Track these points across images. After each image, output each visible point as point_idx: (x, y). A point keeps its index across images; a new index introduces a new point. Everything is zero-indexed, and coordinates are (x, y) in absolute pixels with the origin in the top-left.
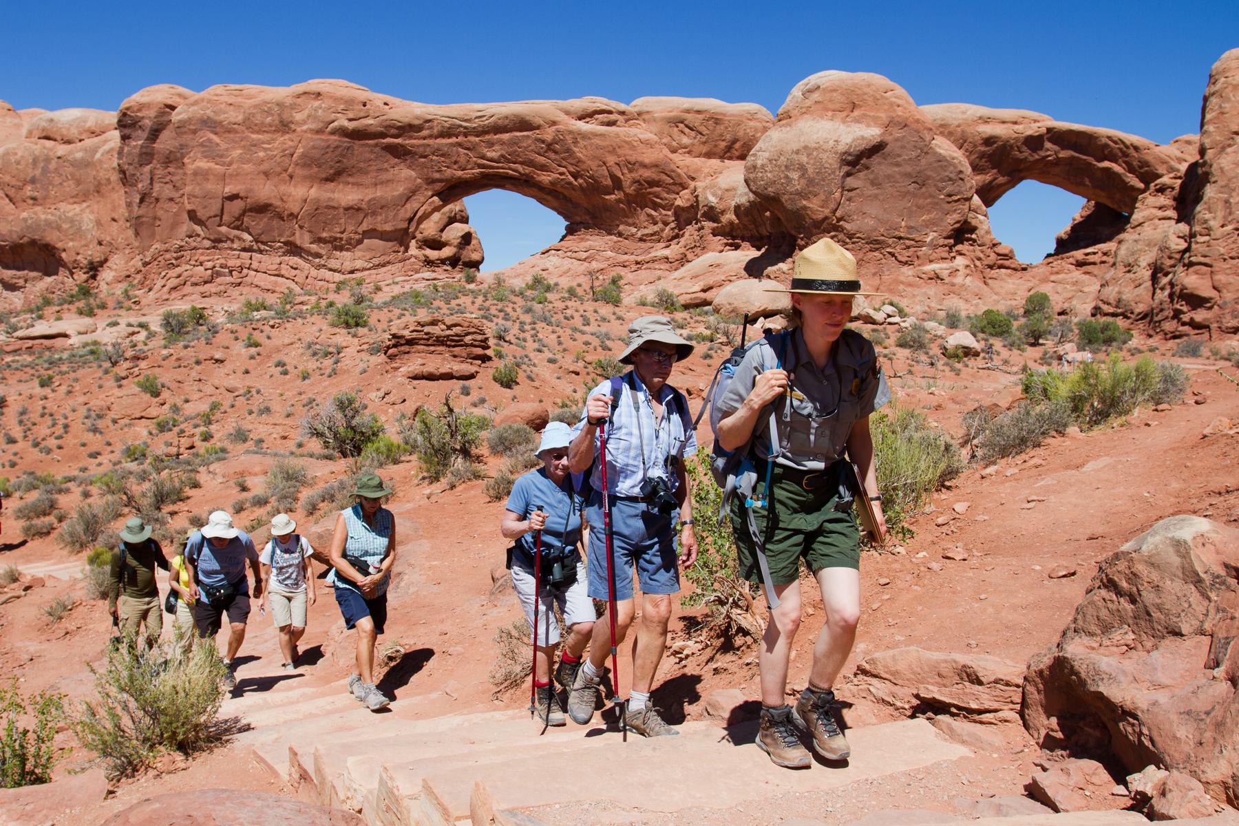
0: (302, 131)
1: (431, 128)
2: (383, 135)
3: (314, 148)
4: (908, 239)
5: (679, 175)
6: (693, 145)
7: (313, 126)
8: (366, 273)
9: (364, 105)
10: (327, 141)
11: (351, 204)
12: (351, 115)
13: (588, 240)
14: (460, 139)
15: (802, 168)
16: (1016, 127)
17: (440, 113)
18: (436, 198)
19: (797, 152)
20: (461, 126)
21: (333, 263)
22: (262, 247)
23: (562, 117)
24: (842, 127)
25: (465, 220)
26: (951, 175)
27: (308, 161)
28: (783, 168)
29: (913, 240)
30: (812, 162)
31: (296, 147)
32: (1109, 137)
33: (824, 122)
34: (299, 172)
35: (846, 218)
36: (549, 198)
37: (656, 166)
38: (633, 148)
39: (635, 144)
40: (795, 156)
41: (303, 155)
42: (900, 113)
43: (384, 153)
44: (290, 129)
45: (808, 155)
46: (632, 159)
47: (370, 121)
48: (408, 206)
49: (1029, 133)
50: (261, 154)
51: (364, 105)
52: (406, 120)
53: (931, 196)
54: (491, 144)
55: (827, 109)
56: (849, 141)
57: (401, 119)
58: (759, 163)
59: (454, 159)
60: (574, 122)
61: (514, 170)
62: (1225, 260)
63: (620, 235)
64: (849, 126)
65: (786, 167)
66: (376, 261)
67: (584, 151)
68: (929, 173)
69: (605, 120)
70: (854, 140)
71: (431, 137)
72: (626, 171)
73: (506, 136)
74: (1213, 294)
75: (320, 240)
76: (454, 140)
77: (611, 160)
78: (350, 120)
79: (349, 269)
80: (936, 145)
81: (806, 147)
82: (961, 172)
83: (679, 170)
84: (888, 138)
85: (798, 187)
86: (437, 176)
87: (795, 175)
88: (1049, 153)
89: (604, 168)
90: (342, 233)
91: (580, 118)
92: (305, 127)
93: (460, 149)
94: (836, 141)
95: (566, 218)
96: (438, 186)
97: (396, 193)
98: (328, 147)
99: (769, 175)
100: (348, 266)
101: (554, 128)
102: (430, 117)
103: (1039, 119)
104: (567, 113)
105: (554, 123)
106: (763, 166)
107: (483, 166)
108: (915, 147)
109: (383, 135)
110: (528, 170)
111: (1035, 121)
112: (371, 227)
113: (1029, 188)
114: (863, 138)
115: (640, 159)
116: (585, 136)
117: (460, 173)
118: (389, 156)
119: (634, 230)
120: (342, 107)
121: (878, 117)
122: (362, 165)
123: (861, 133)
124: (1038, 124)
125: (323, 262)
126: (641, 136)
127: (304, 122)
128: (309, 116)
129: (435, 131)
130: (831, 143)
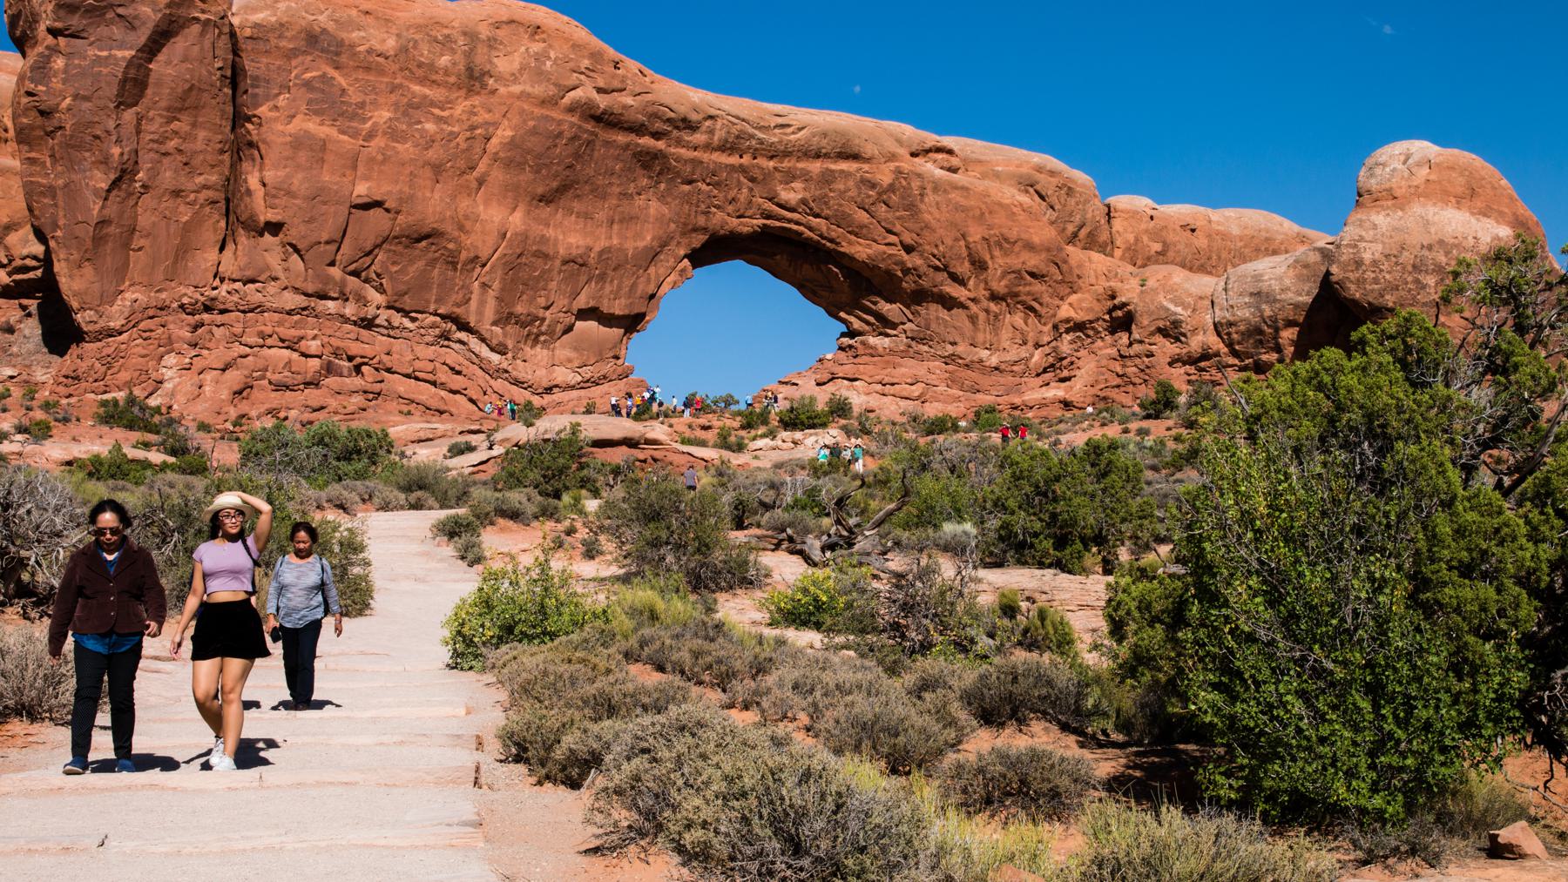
0: (511, 95)
1: (711, 132)
2: (638, 129)
3: (534, 132)
7: (539, 90)
10: (560, 123)
11: (574, 252)
13: (901, 365)
14: (746, 160)
19: (1430, 248)
20: (752, 136)
21: (521, 371)
22: (397, 319)
27: (516, 157)
28: (1410, 269)
31: (496, 125)
34: (498, 175)
40: (1426, 253)
41: (512, 144)
44: (484, 86)
45: (1447, 254)
46: (1013, 235)
47: (629, 101)
48: (652, 270)
50: (430, 127)
54: (790, 177)
57: (674, 107)
58: (1367, 256)
59: (732, 194)
61: (811, 229)
63: (950, 359)
65: (1414, 266)
66: (587, 372)
67: (933, 210)
71: (708, 147)
72: (997, 253)
73: (816, 167)
75: (504, 319)
76: (734, 160)
77: (976, 234)
78: (600, 90)
79: (545, 384)
81: (1441, 242)
86: (701, 221)
89: (962, 243)
92: (516, 89)
98: (560, 134)
99: (1388, 276)
100: (541, 376)
101: (892, 165)
102: (713, 112)
106: (1375, 263)
109: (638, 129)
110: (836, 232)
115: (1024, 236)
119: (984, 354)
125: (505, 365)
127: (514, 78)
128: (522, 69)
129: (716, 138)
130: (1471, 241)
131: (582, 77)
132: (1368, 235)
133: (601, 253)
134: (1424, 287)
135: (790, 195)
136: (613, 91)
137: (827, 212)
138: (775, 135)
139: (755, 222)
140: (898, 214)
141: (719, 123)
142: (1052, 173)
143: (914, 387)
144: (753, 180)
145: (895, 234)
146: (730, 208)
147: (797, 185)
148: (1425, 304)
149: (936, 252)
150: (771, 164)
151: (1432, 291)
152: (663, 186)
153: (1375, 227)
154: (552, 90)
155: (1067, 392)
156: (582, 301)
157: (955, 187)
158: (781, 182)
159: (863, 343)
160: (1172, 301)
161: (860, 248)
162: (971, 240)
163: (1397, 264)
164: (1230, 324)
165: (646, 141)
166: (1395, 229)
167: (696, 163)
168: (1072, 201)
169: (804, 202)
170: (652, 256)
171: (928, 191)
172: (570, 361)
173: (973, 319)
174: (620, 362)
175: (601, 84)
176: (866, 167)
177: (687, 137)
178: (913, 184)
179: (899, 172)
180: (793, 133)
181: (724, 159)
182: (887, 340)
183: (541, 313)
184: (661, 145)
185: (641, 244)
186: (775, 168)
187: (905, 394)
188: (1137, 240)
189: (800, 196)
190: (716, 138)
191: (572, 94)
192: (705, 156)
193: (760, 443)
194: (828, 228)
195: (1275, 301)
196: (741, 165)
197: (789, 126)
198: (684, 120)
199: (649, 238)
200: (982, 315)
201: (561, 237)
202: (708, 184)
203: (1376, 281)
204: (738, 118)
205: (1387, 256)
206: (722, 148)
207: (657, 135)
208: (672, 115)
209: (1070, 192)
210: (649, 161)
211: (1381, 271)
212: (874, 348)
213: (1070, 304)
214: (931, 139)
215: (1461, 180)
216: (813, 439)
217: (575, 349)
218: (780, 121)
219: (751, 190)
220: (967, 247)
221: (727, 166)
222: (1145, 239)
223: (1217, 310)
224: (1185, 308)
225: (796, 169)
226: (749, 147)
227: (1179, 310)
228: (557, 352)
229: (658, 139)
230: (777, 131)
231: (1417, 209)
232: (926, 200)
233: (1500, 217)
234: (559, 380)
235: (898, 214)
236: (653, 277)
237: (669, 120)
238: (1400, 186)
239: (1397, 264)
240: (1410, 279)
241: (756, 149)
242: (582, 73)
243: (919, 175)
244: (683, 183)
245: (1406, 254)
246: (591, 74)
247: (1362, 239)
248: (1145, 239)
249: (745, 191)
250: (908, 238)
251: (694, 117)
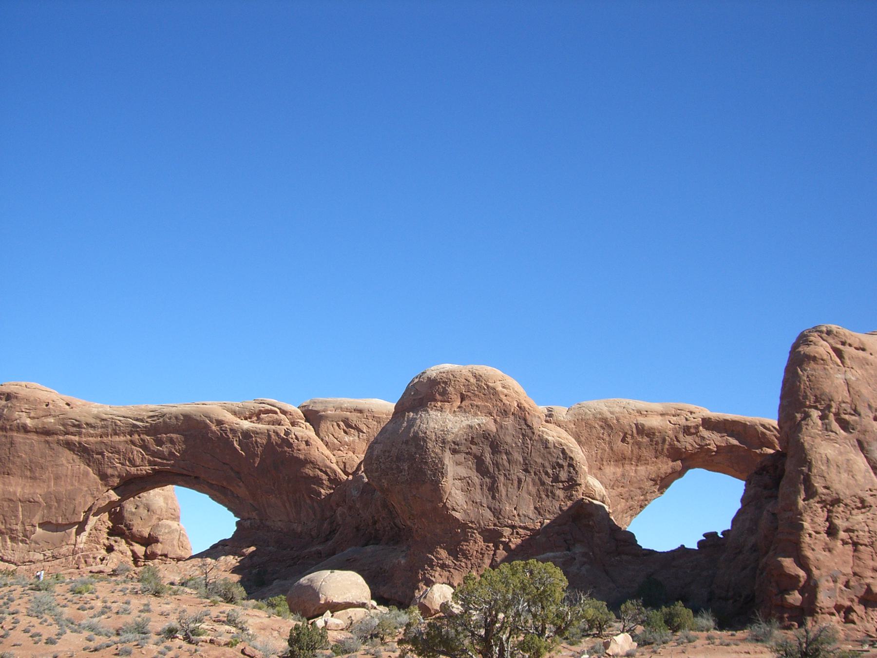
4: (520, 527)
5: (335, 472)
6: (354, 441)
8: (39, 564)
9: (47, 405)
12: (32, 415)
16: (674, 419)
17: (115, 412)
18: (111, 492)
23: (229, 417)
24: (450, 416)
25: (176, 518)
26: (560, 462)
29: (525, 528)
32: (763, 426)
33: (431, 412)
35: (456, 507)
36: (218, 494)
37: (312, 462)
38: (290, 445)
39: (291, 441)
40: (404, 446)
42: (506, 402)
43: (61, 449)
49: (683, 422)
51: (47, 405)
52: (83, 420)
53: (543, 483)
55: (436, 400)
56: (455, 430)
57: (78, 418)
60: (239, 420)
62: (810, 535)
64: (456, 416)
68: (539, 460)
69: (270, 419)
70: (460, 429)
74: (802, 573)
80: (543, 432)
82: (571, 458)
83: (334, 466)
84: (493, 427)
88: (708, 442)
90: (17, 524)
91: (246, 419)
93: (133, 447)
94: (442, 431)
95: (236, 515)
96: (116, 481)
97: (70, 488)
102: (105, 416)
103: (694, 410)
104: (235, 413)
105: (220, 423)
107: (155, 464)
108: (523, 435)
111: (691, 413)
112: (46, 520)
113: (697, 476)
114: (471, 427)
116: (247, 434)
117: (133, 470)
118: (67, 453)
120: (27, 406)
121: (485, 406)
122: (42, 461)
123: (469, 423)
124: (694, 415)
126: (299, 434)
138: (147, 422)
148: (402, 483)
178: (231, 436)
181: (117, 439)
183: (14, 527)
184: (77, 438)
192: (105, 439)
198: (87, 424)
202: (112, 453)
204: (124, 417)
210: (69, 445)
218: (151, 414)
230: (149, 420)
234: (31, 558)
237: (74, 426)
239: (389, 457)
240: (394, 466)
242: (22, 412)
249: (135, 453)
251: (92, 421)
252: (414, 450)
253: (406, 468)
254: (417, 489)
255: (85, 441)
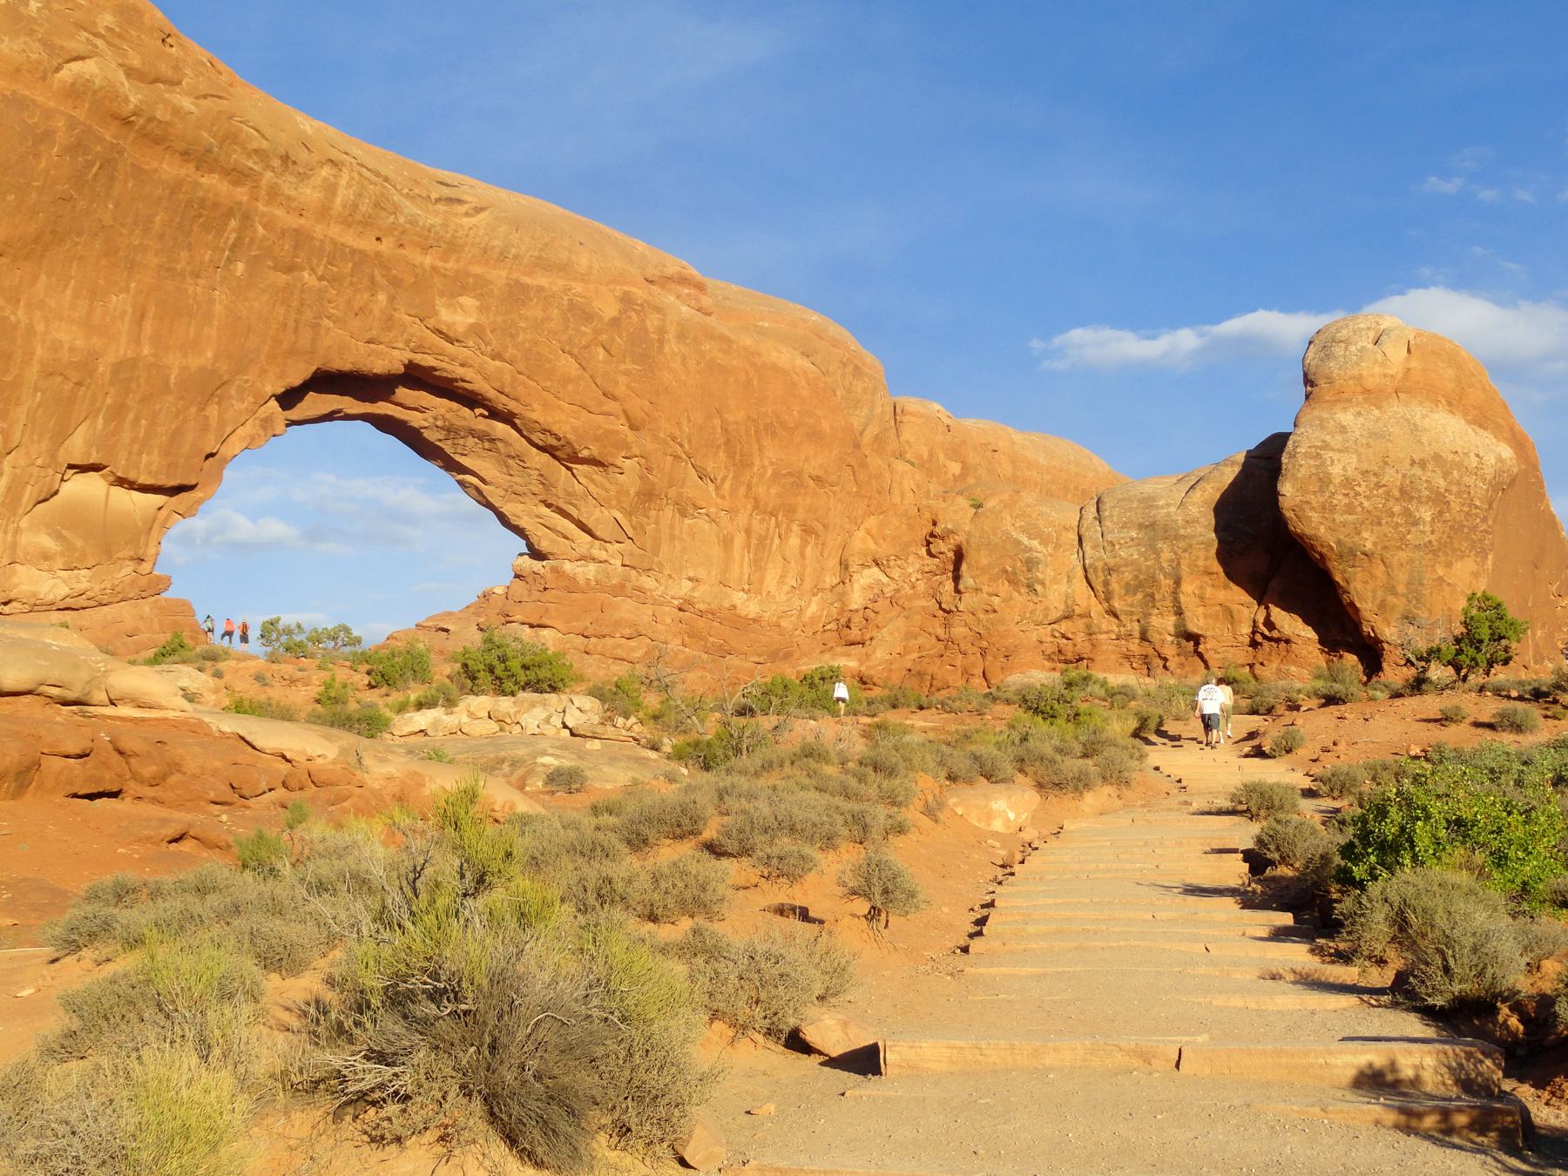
1: (331, 189)
2: (203, 159)
10: (48, 114)
14: (386, 247)
15: (1438, 500)
19: (1423, 464)
28: (1396, 493)
30: (1454, 489)
40: (1417, 471)
45: (1446, 475)
47: (187, 103)
57: (268, 131)
58: (1336, 470)
65: (1402, 490)
66: (82, 580)
81: (1437, 457)
85: (1433, 538)
87: (1426, 514)
89: (717, 422)
99: (1366, 504)
106: (1348, 482)
109: (203, 159)
130: (1474, 461)
131: (99, 42)
132: (1336, 441)
133: (117, 368)
134: (1416, 523)
135: (460, 315)
136: (156, 80)
137: (510, 352)
138: (437, 213)
139: (396, 353)
140: (623, 367)
141: (344, 179)
142: (835, 343)
143: (633, 643)
144: (396, 282)
145: (614, 398)
146: (356, 323)
147: (468, 301)
148: (1417, 547)
149: (677, 433)
150: (428, 261)
151: (1428, 528)
152: (240, 267)
153: (1343, 429)
154: (37, 53)
155: (861, 662)
156: (77, 447)
157: (711, 336)
158: (442, 294)
159: (555, 570)
160: (1023, 530)
161: (563, 417)
162: (730, 418)
163: (1378, 486)
164: (1109, 570)
165: (212, 182)
166: (1372, 435)
167: (300, 238)
168: (859, 386)
169: (476, 330)
170: (209, 388)
171: (671, 336)
172: (47, 556)
173: (727, 543)
174: (145, 567)
175: (136, 62)
176: (578, 288)
177: (288, 185)
178: (649, 324)
179: (627, 300)
180: (467, 214)
182: (592, 567)
184: (241, 194)
185: (195, 362)
186: (434, 269)
187: (620, 653)
188: (931, 454)
189: (472, 320)
190: (338, 200)
191: (76, 66)
192: (319, 230)
193: (423, 719)
194: (514, 379)
195: (1178, 537)
196: (378, 254)
197: (459, 201)
199: (210, 354)
200: (739, 540)
201: (40, 328)
202: (321, 278)
203: (1350, 509)
205: (1365, 473)
206: (350, 219)
207: (238, 175)
208: (265, 144)
209: (858, 372)
211: (1357, 494)
212: (573, 579)
213: (868, 532)
214: (674, 265)
215: (1450, 373)
216: (539, 713)
217: (59, 537)
218: (446, 192)
219: (392, 299)
220: (725, 431)
221: (353, 251)
222: (941, 456)
223: (1087, 547)
224: (1044, 542)
225: (468, 274)
226: (393, 227)
227: (1035, 543)
228: (24, 539)
229: (236, 183)
231: (1396, 409)
232: (667, 349)
233: (1497, 431)
235: (623, 367)
236: (214, 423)
238: (1372, 372)
239: (1378, 486)
241: (403, 232)
243: (658, 310)
244: (275, 268)
245: (1390, 471)
246: (117, 41)
247: (1326, 446)
248: (941, 456)
250: (637, 406)
251: (301, 155)
252: (1442, 484)
253: (1429, 519)
254: (1449, 565)
255: (263, 215)
